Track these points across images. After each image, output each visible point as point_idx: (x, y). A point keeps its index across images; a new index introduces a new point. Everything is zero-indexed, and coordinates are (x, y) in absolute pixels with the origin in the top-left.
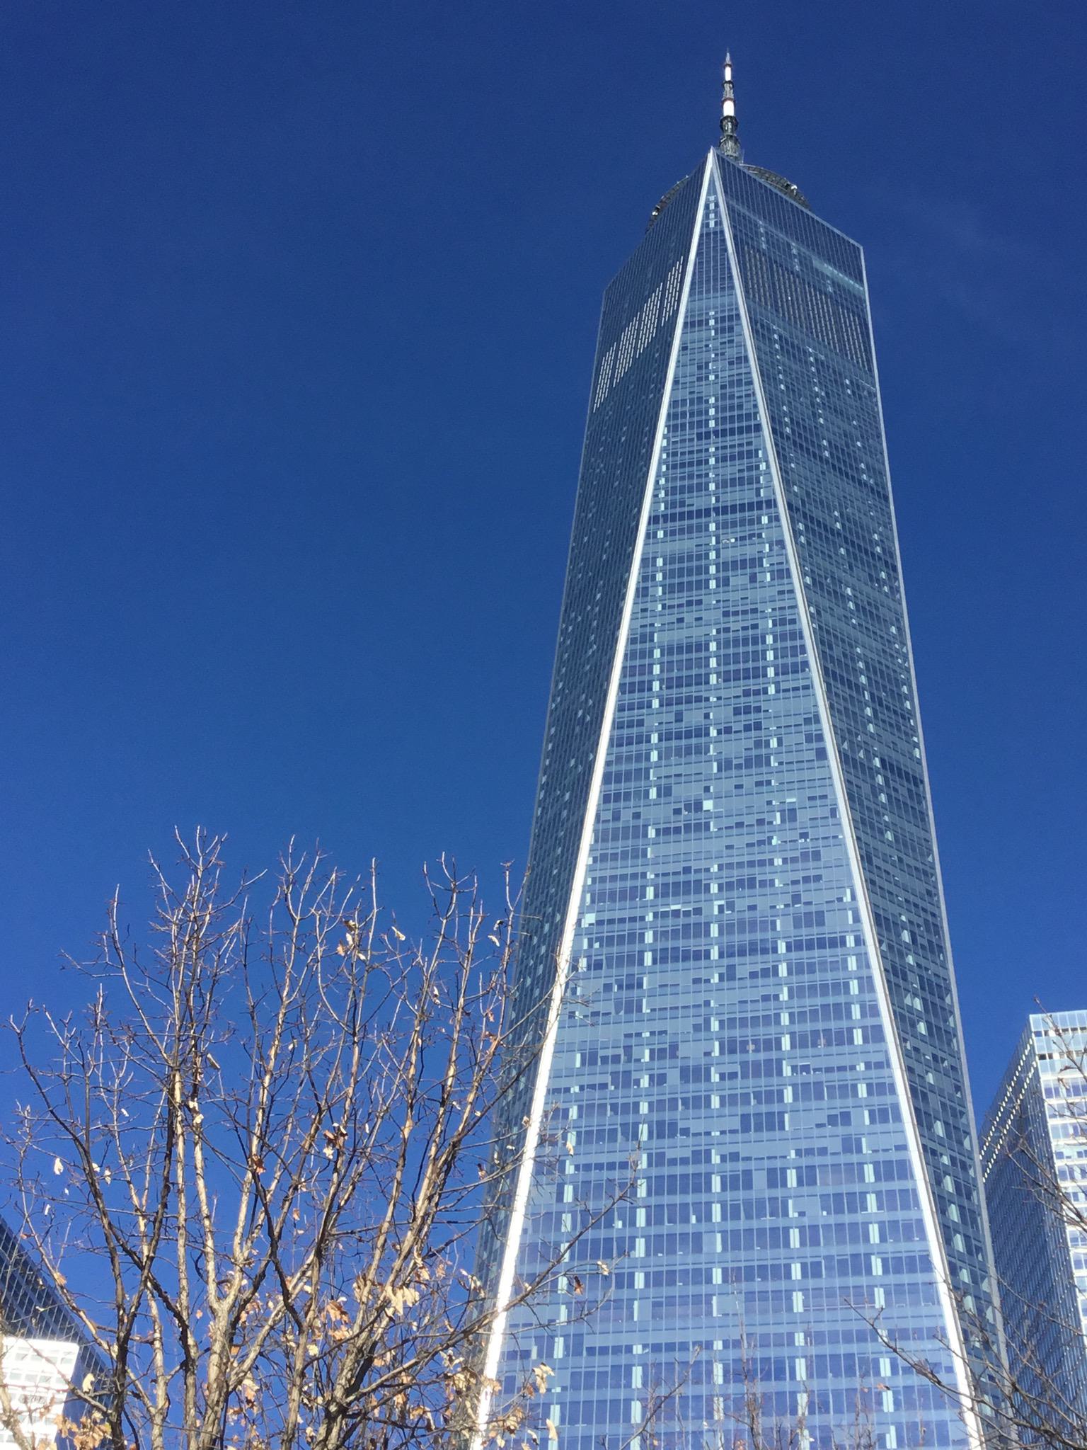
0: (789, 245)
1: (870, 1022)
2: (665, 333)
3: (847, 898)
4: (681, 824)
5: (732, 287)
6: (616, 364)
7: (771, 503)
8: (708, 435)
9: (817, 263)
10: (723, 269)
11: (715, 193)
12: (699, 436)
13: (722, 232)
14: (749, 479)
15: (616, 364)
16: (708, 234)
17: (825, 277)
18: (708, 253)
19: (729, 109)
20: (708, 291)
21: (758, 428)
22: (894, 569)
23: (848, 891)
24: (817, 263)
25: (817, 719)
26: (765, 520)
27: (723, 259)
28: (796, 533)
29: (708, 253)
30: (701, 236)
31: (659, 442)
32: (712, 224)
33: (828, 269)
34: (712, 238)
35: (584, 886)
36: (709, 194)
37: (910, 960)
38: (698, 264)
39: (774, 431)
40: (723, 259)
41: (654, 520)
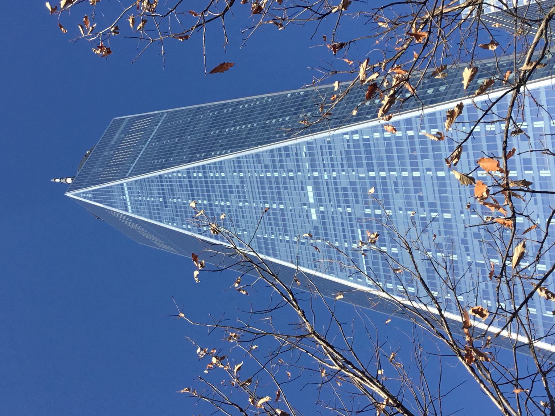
0: (104, 156)
1: (402, 127)
3: (347, 137)
4: (322, 226)
5: (111, 186)
8: (165, 202)
9: (113, 143)
10: (106, 191)
11: (79, 193)
12: (166, 206)
13: (93, 191)
14: (180, 180)
16: (94, 198)
18: (101, 198)
20: (114, 199)
21: (160, 176)
22: (224, 105)
23: (345, 136)
24: (113, 143)
25: (272, 151)
26: (195, 175)
27: (103, 191)
29: (101, 198)
30: (95, 201)
32: (90, 196)
33: (117, 136)
34: (96, 195)
35: (354, 282)
36: (80, 197)
40: (103, 191)
41: (200, 232)
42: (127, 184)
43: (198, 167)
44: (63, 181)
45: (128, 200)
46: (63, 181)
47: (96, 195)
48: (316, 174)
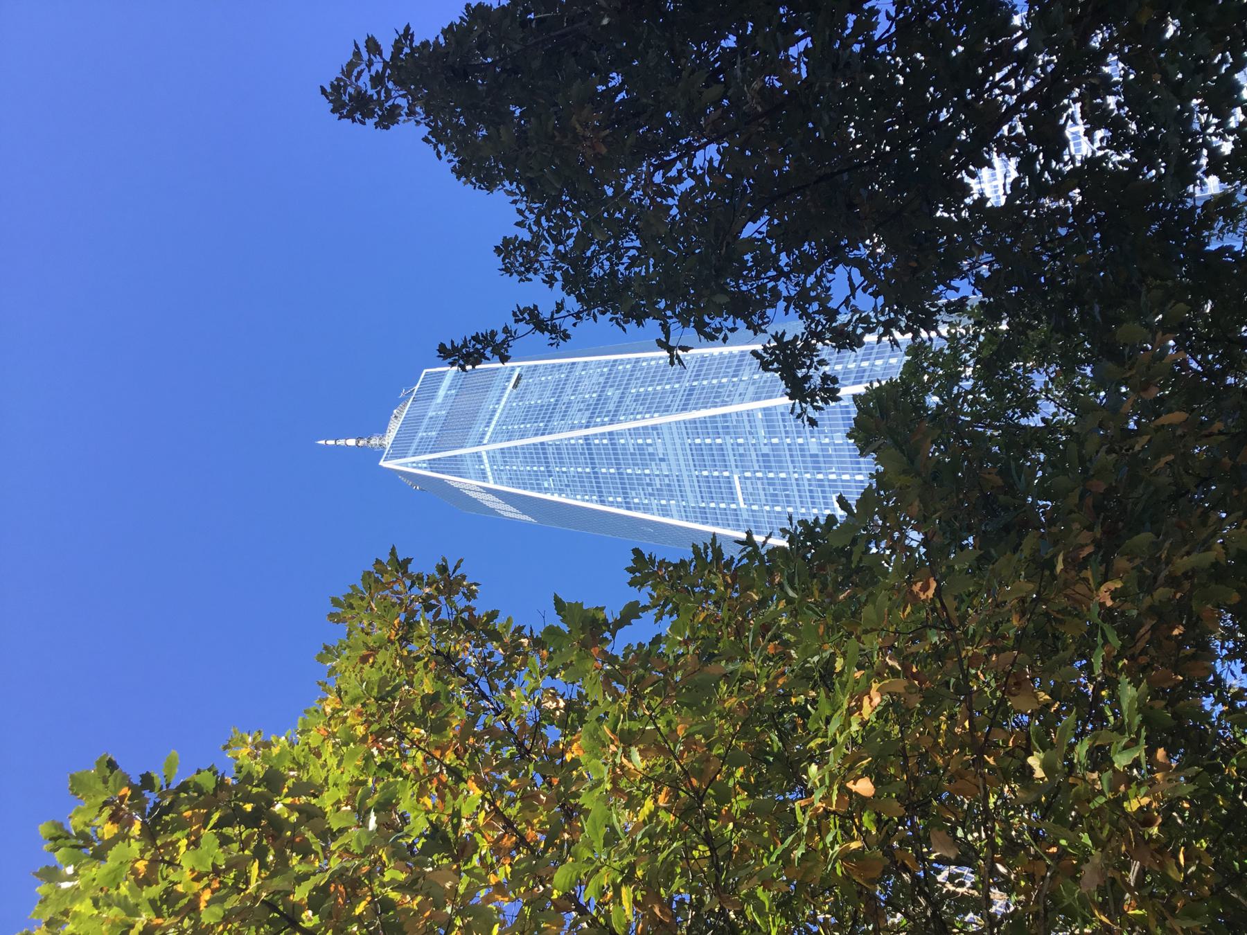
2: (489, 491)
6: (509, 511)
7: (586, 438)
9: (439, 400)
15: (509, 511)
17: (446, 396)
19: (352, 442)
21: (542, 444)
22: (615, 361)
24: (439, 400)
26: (597, 441)
28: (603, 424)
31: (556, 498)
33: (442, 392)
37: (852, 366)
38: (448, 473)
39: (543, 434)
41: (602, 502)
42: (488, 452)
43: (603, 434)
44: (341, 442)
45: (488, 469)
46: (341, 442)
47: (432, 465)
48: (775, 441)
